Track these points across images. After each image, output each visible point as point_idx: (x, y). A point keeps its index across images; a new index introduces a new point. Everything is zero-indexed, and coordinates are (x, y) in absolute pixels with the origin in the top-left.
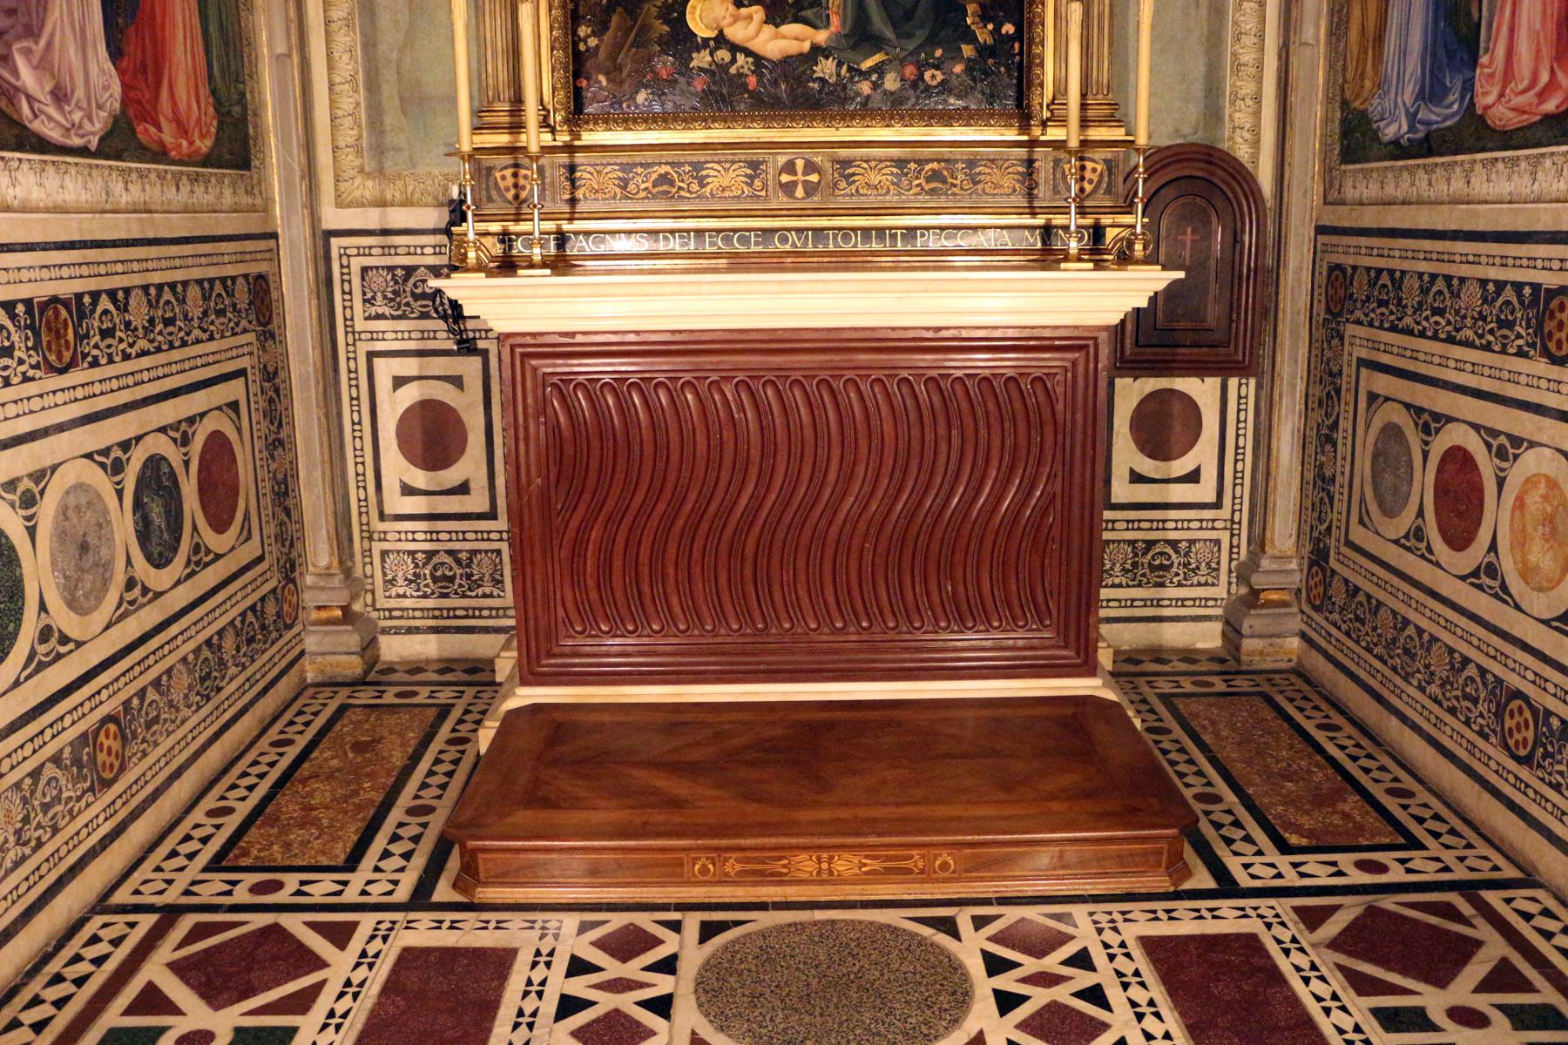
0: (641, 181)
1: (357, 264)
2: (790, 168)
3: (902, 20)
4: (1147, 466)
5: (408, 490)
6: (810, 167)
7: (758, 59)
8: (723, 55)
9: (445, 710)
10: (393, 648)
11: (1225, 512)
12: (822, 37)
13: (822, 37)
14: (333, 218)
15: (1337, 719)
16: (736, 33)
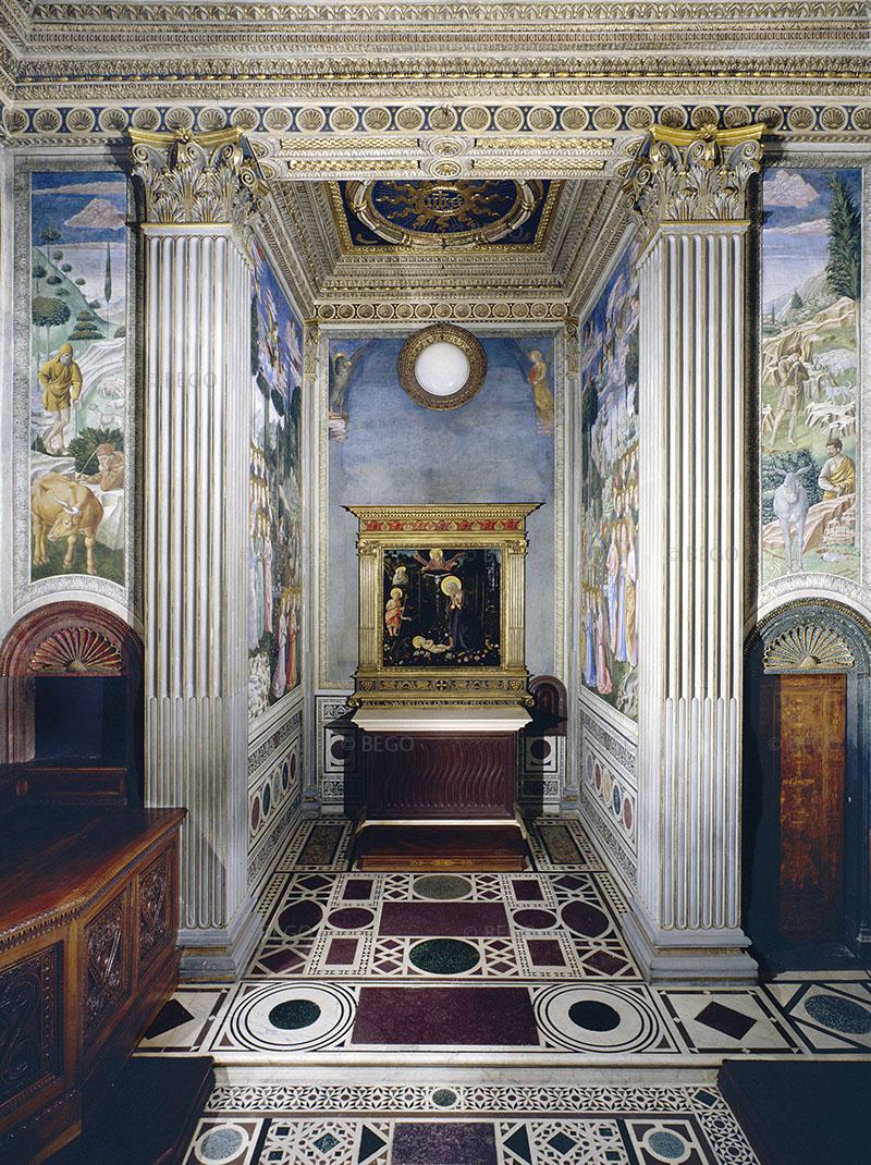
0: (400, 685)
1: (323, 704)
2: (439, 682)
3: (469, 645)
4: (535, 760)
5: (333, 765)
6: (444, 683)
7: (432, 653)
8: (422, 652)
9: (343, 827)
10: (326, 810)
11: (558, 773)
12: (448, 648)
13: (448, 648)
14: (317, 692)
15: (582, 833)
16: (425, 647)
